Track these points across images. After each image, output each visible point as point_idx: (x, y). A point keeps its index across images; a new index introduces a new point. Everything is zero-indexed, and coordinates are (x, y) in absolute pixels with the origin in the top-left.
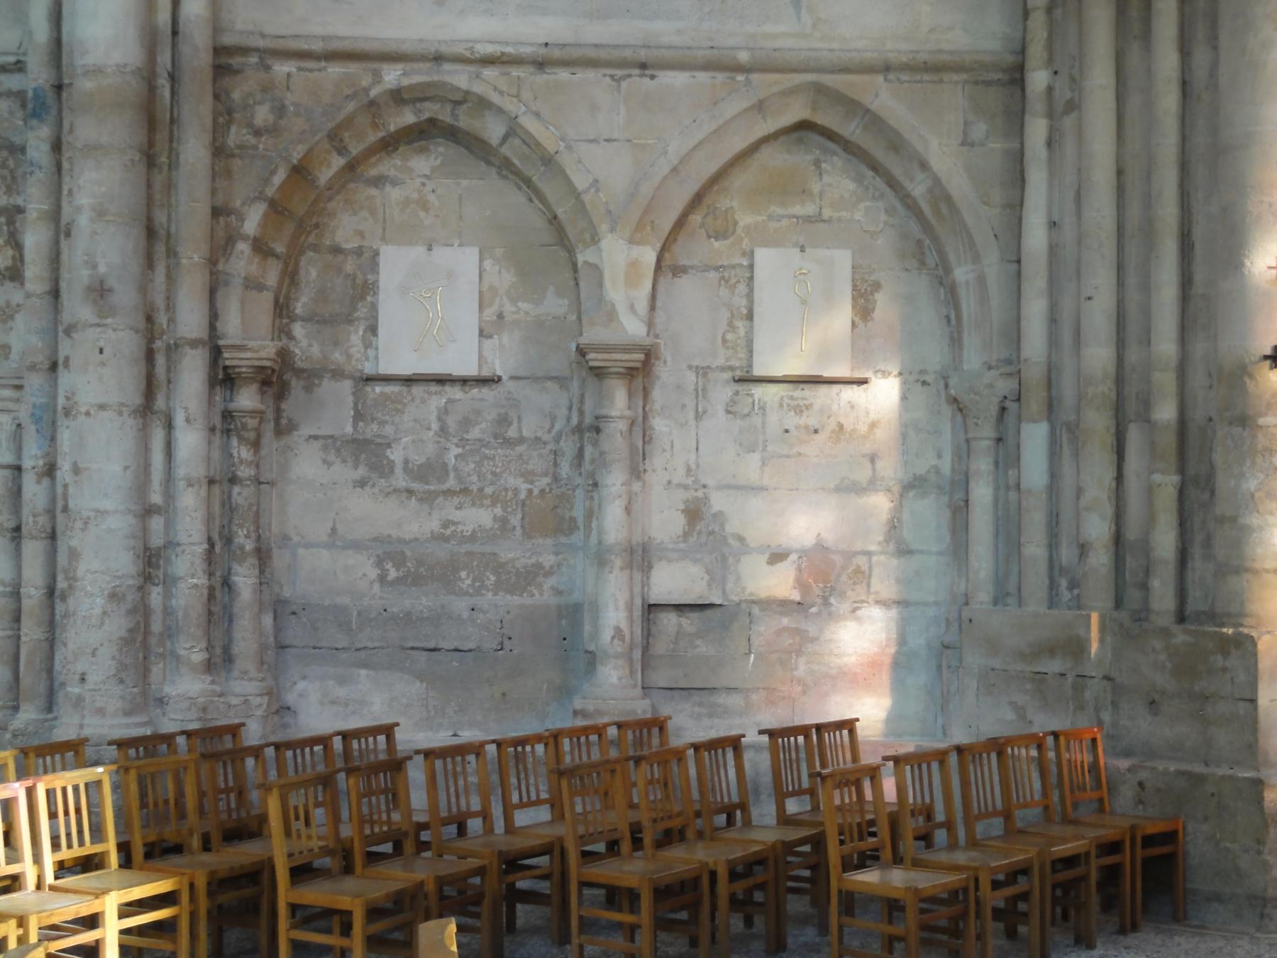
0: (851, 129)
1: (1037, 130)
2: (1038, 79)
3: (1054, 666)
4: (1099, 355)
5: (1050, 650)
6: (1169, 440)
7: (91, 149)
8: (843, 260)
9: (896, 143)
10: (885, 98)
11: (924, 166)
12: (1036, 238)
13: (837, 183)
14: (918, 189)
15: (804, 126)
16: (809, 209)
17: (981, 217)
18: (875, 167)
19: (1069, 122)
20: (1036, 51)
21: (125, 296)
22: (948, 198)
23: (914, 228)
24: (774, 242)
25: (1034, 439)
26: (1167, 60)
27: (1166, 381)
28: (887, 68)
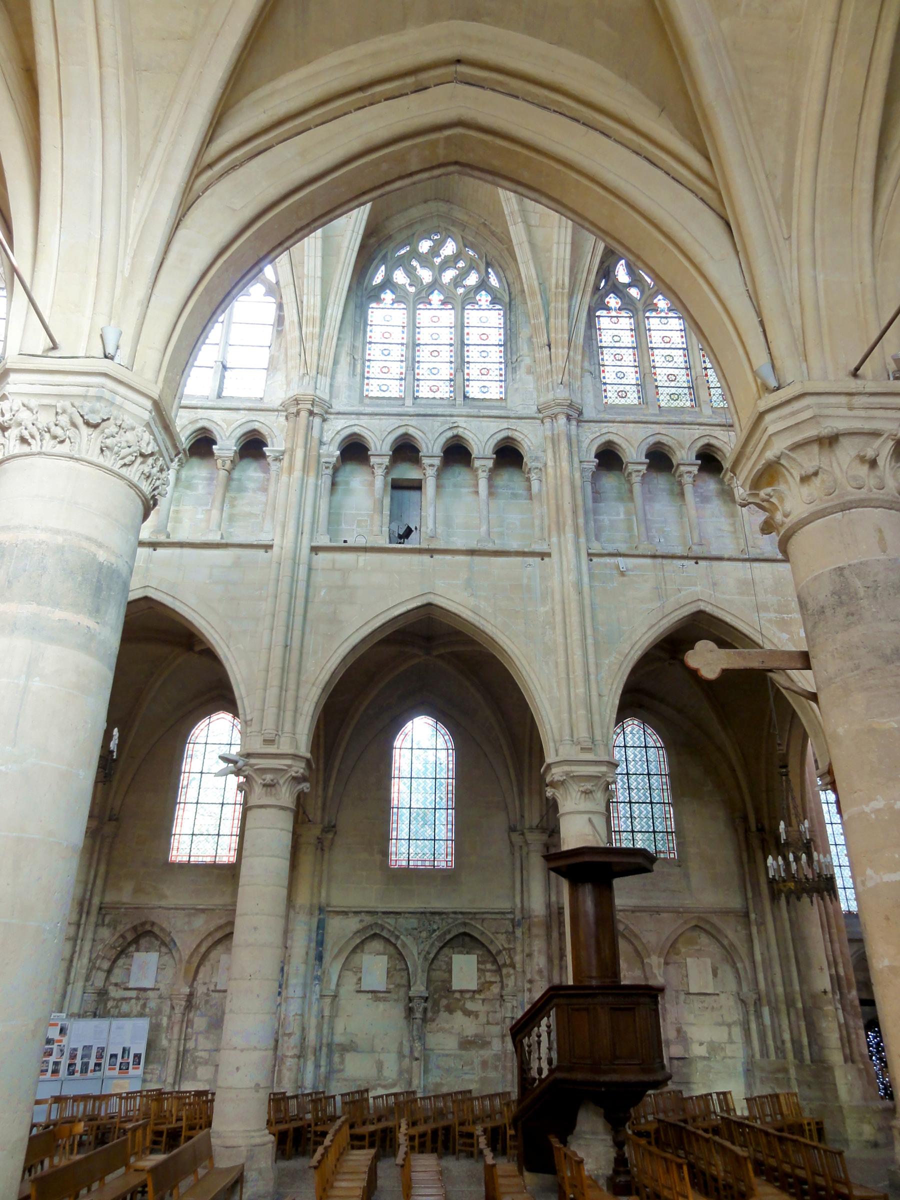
0: (707, 927)
1: (754, 930)
2: (753, 916)
3: (780, 1076)
4: (780, 989)
5: (778, 1071)
6: (801, 1013)
7: (536, 936)
8: (708, 961)
9: (719, 931)
10: (715, 919)
11: (727, 937)
12: (758, 958)
13: (704, 939)
14: (726, 943)
15: (696, 926)
16: (698, 947)
17: (743, 950)
18: (714, 937)
19: (762, 928)
20: (751, 908)
21: (545, 973)
22: (734, 946)
23: (725, 953)
24: (690, 956)
25: (766, 1011)
26: (785, 915)
27: (798, 996)
28: (715, 912)
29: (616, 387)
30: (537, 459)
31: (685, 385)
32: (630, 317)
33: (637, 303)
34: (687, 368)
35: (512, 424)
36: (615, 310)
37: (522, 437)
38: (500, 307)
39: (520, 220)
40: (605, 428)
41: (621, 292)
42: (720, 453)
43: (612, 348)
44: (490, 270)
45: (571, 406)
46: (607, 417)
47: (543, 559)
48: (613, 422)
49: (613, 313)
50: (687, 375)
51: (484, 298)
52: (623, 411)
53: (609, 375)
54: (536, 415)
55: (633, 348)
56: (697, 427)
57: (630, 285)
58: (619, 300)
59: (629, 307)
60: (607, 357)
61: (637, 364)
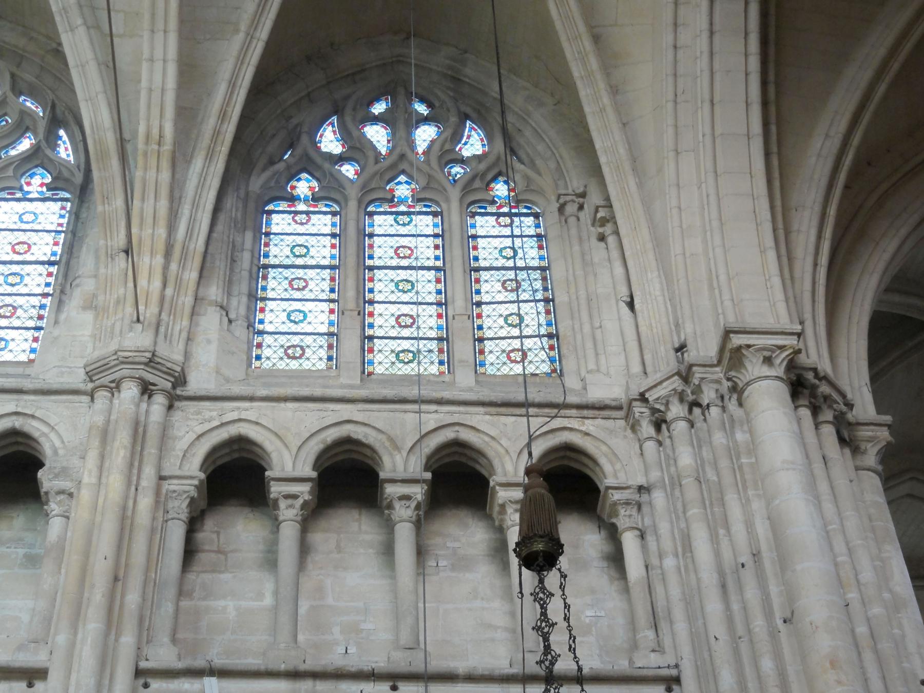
29: (282, 339)
30: (64, 472)
31: (433, 334)
32: (334, 214)
33: (348, 186)
34: (439, 304)
35: (27, 404)
36: (306, 200)
37: (45, 429)
38: (67, 195)
39: (79, 21)
40: (231, 411)
41: (319, 167)
42: (483, 461)
43: (287, 267)
44: (62, 132)
45: (152, 362)
46: (236, 390)
47: (30, 685)
48: (252, 399)
49: (301, 207)
50: (440, 316)
51: (37, 182)
52: (283, 380)
53: (274, 317)
54: (82, 386)
55: (332, 267)
56: (433, 407)
57: (341, 159)
58: (315, 184)
59: (333, 195)
60: (275, 284)
61: (334, 296)
